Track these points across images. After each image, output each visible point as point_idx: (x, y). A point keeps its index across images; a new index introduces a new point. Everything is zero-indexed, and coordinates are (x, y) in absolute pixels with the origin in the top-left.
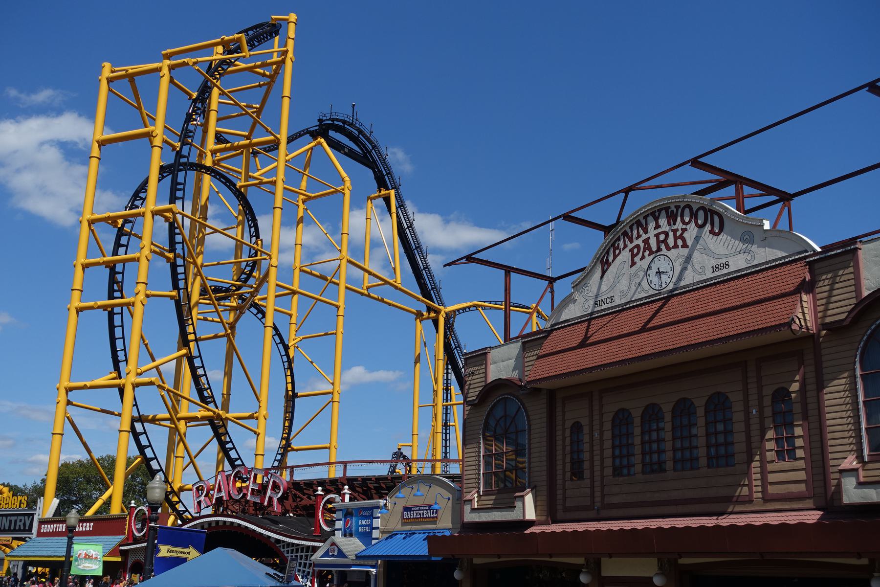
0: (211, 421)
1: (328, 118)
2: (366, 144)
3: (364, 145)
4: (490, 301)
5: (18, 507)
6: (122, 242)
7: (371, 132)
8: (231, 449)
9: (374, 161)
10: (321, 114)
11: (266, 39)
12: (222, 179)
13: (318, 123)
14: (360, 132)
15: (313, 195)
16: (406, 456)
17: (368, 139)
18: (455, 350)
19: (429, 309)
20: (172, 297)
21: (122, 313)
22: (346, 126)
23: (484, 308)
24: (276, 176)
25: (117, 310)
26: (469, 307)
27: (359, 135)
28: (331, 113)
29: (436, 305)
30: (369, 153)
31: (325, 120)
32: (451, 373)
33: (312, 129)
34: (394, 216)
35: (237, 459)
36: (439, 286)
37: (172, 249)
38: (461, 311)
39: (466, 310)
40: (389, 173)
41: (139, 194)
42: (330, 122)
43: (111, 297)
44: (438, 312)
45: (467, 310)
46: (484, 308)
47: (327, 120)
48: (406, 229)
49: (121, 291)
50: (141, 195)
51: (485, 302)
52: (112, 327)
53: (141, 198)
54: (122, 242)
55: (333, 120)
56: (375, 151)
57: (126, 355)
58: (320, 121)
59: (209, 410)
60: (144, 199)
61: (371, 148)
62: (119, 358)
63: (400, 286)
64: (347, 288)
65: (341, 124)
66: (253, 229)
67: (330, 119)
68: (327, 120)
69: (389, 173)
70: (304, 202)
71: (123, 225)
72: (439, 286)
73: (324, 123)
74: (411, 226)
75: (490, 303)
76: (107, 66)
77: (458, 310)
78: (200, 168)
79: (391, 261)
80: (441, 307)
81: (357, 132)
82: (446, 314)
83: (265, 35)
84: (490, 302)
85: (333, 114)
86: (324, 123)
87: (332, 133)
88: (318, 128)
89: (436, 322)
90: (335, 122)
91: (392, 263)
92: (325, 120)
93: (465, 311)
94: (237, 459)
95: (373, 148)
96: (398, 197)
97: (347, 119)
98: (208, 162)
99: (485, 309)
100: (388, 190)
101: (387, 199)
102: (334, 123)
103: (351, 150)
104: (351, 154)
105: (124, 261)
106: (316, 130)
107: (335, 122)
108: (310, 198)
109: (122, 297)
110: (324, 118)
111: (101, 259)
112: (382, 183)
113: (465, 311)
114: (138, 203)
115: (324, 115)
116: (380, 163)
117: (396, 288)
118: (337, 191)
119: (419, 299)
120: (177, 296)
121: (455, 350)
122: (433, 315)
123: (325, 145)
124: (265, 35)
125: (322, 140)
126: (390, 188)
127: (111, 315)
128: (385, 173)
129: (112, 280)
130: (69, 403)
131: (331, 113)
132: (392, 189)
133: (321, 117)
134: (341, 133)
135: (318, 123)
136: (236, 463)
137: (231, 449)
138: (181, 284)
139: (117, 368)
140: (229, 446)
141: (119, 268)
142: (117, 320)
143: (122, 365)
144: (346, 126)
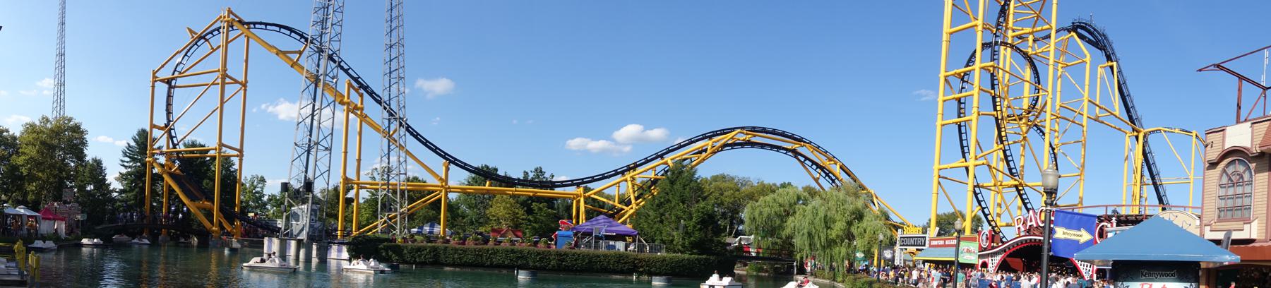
19: (1134, 130)
20: (994, 115)
25: (963, 124)
41: (971, 61)
43: (959, 117)
52: (960, 133)
60: (974, 62)
63: (1118, 116)
64: (1088, 117)
71: (964, 76)
89: (1137, 138)
98: (1010, 41)
105: (965, 97)
111: (953, 96)
117: (1116, 117)
119: (1128, 124)
122: (1136, 134)
127: (960, 127)
129: (960, 109)
138: (998, 108)
139: (964, 157)
142: (963, 130)
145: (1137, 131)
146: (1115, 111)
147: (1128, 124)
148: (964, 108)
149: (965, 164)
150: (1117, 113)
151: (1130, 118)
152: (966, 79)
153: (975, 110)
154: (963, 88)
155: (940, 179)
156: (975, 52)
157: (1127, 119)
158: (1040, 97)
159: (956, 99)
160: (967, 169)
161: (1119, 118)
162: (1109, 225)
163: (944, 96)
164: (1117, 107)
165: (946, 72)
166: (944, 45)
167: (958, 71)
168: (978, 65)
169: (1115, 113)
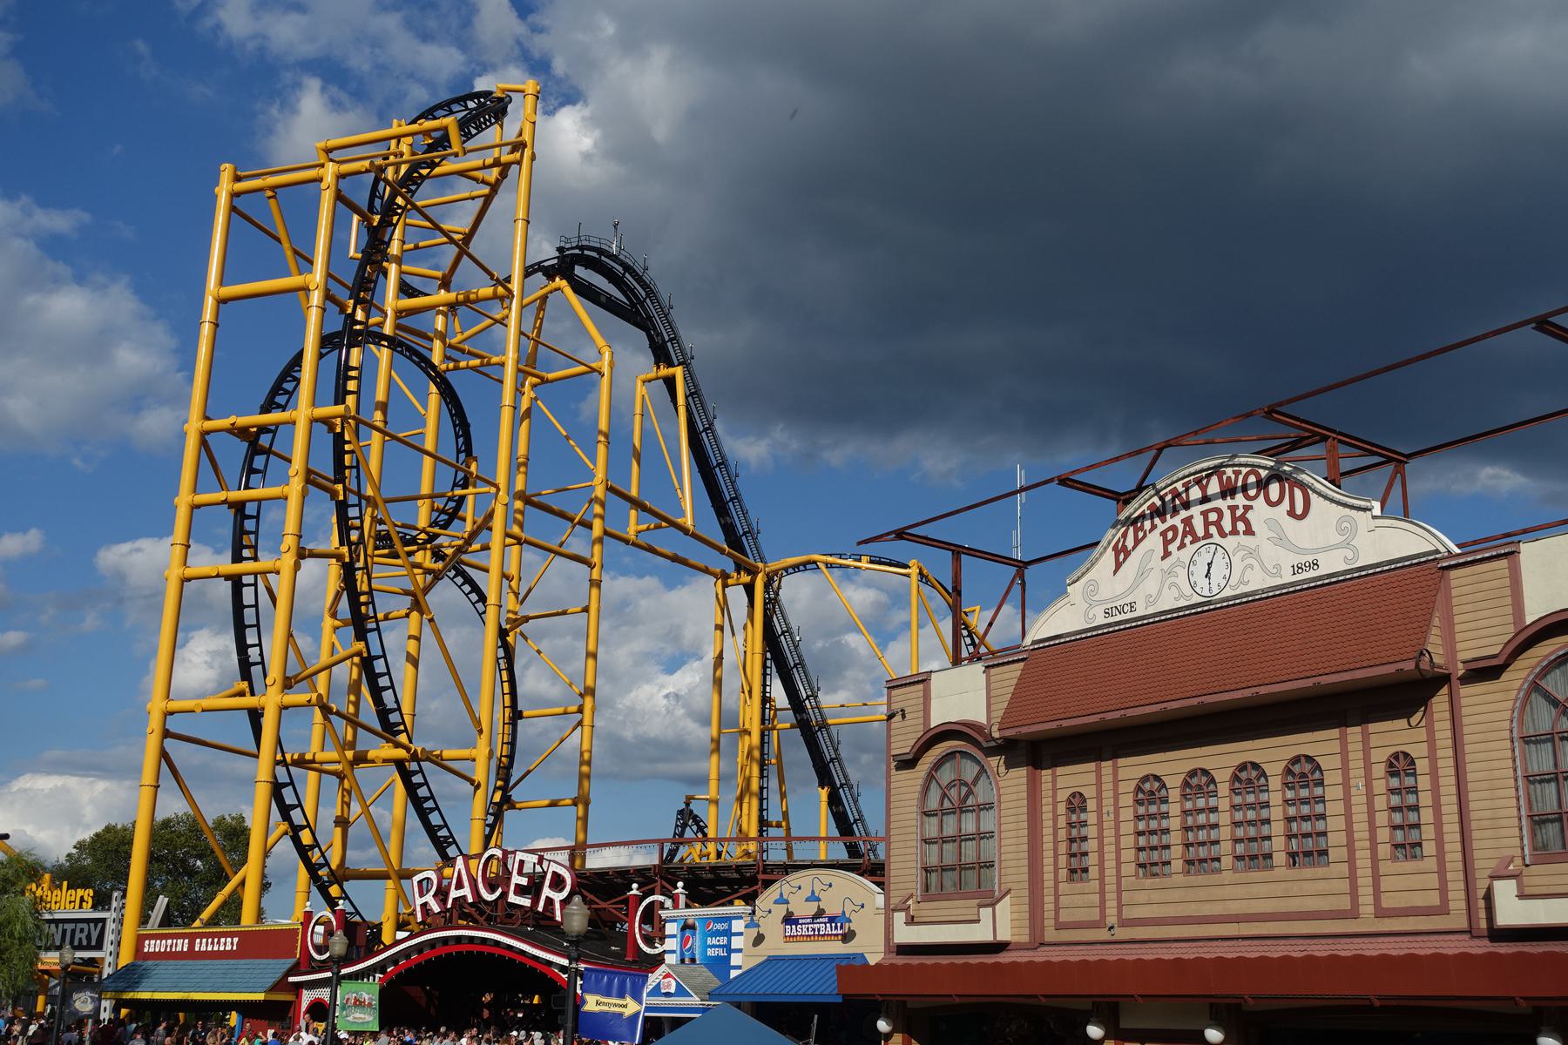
0: (399, 764)
1: (574, 245)
2: (635, 288)
3: (632, 291)
4: (841, 555)
5: (62, 908)
6: (255, 466)
7: (646, 269)
8: (432, 810)
9: (650, 318)
10: (563, 239)
11: (488, 124)
12: (414, 358)
13: (557, 254)
14: (627, 268)
15: (551, 376)
16: (697, 816)
17: (639, 280)
18: (782, 637)
20: (339, 557)
21: (255, 585)
22: (603, 258)
23: (829, 566)
24: (504, 355)
25: (247, 580)
26: (805, 564)
27: (625, 273)
28: (579, 237)
29: (751, 561)
30: (642, 303)
31: (568, 249)
32: (771, 668)
33: (546, 264)
34: (682, 410)
35: (440, 827)
36: (755, 529)
37: (340, 478)
38: (790, 570)
39: (798, 569)
40: (674, 339)
42: (577, 251)
44: (753, 572)
45: (802, 568)
46: (829, 566)
47: (572, 248)
48: (701, 433)
49: (255, 548)
50: (286, 386)
51: (831, 555)
53: (286, 392)
54: (255, 466)
55: (582, 248)
56: (651, 301)
57: (261, 654)
58: (560, 250)
59: (398, 745)
60: (291, 394)
61: (644, 294)
62: (251, 660)
63: (691, 528)
65: (594, 254)
66: (461, 440)
67: (577, 247)
68: (572, 248)
69: (675, 339)
70: (534, 386)
72: (755, 529)
73: (567, 252)
74: (710, 428)
75: (840, 558)
76: (227, 170)
77: (786, 569)
78: (378, 338)
79: (677, 486)
80: (760, 565)
81: (620, 269)
82: (767, 575)
83: (487, 117)
84: (841, 556)
85: (582, 238)
86: (567, 252)
87: (579, 271)
88: (556, 261)
90: (586, 252)
91: (679, 490)
92: (568, 249)
93: (797, 570)
94: (440, 827)
95: (648, 295)
96: (690, 377)
97: (603, 247)
99: (831, 567)
100: (670, 364)
101: (670, 382)
102: (583, 252)
103: (610, 297)
104: (610, 305)
105: (260, 501)
106: (553, 265)
107: (586, 252)
108: (544, 381)
109: (255, 559)
110: (568, 246)
111: (222, 496)
112: (661, 355)
113: (797, 570)
114: (281, 399)
115: (568, 240)
116: (659, 321)
117: (685, 531)
118: (593, 370)
120: (347, 555)
121: (782, 637)
122: (746, 578)
123: (568, 291)
124: (487, 117)
125: (564, 283)
126: (676, 363)
128: (667, 338)
129: (239, 532)
130: (166, 734)
131: (579, 237)
132: (678, 365)
133: (563, 244)
134: (594, 270)
135: (557, 254)
136: (439, 834)
137: (432, 810)
139: (246, 674)
140: (430, 804)
141: (251, 509)
143: (256, 671)
144: (603, 258)
145: (749, 572)
146: (683, 514)
147: (722, 551)
148: (256, 533)
149: (248, 701)
150: (688, 521)
151: (729, 530)
152: (264, 440)
153: (289, 541)
154: (252, 471)
155: (169, 742)
156: (298, 359)
157: (719, 538)
158: (470, 499)
159: (232, 505)
160: (255, 715)
161: (694, 536)
162: (668, 903)
163: (195, 490)
164: (688, 505)
165: (207, 418)
166: (206, 329)
167: (242, 421)
168: (303, 410)
169: (680, 521)
